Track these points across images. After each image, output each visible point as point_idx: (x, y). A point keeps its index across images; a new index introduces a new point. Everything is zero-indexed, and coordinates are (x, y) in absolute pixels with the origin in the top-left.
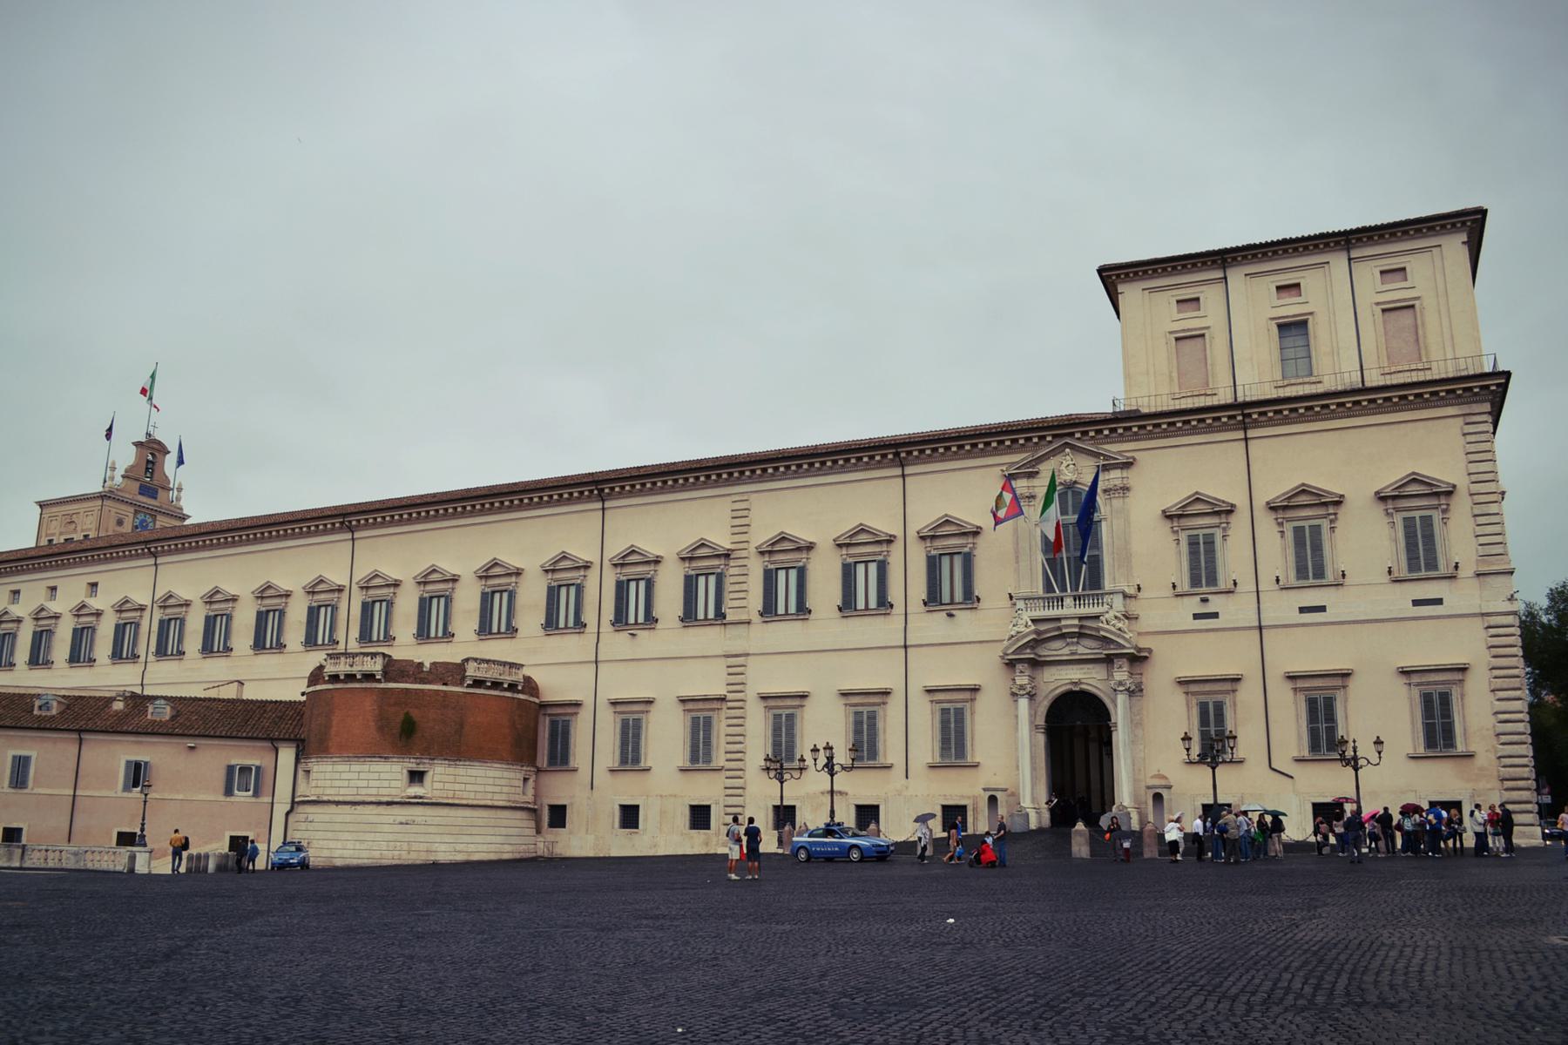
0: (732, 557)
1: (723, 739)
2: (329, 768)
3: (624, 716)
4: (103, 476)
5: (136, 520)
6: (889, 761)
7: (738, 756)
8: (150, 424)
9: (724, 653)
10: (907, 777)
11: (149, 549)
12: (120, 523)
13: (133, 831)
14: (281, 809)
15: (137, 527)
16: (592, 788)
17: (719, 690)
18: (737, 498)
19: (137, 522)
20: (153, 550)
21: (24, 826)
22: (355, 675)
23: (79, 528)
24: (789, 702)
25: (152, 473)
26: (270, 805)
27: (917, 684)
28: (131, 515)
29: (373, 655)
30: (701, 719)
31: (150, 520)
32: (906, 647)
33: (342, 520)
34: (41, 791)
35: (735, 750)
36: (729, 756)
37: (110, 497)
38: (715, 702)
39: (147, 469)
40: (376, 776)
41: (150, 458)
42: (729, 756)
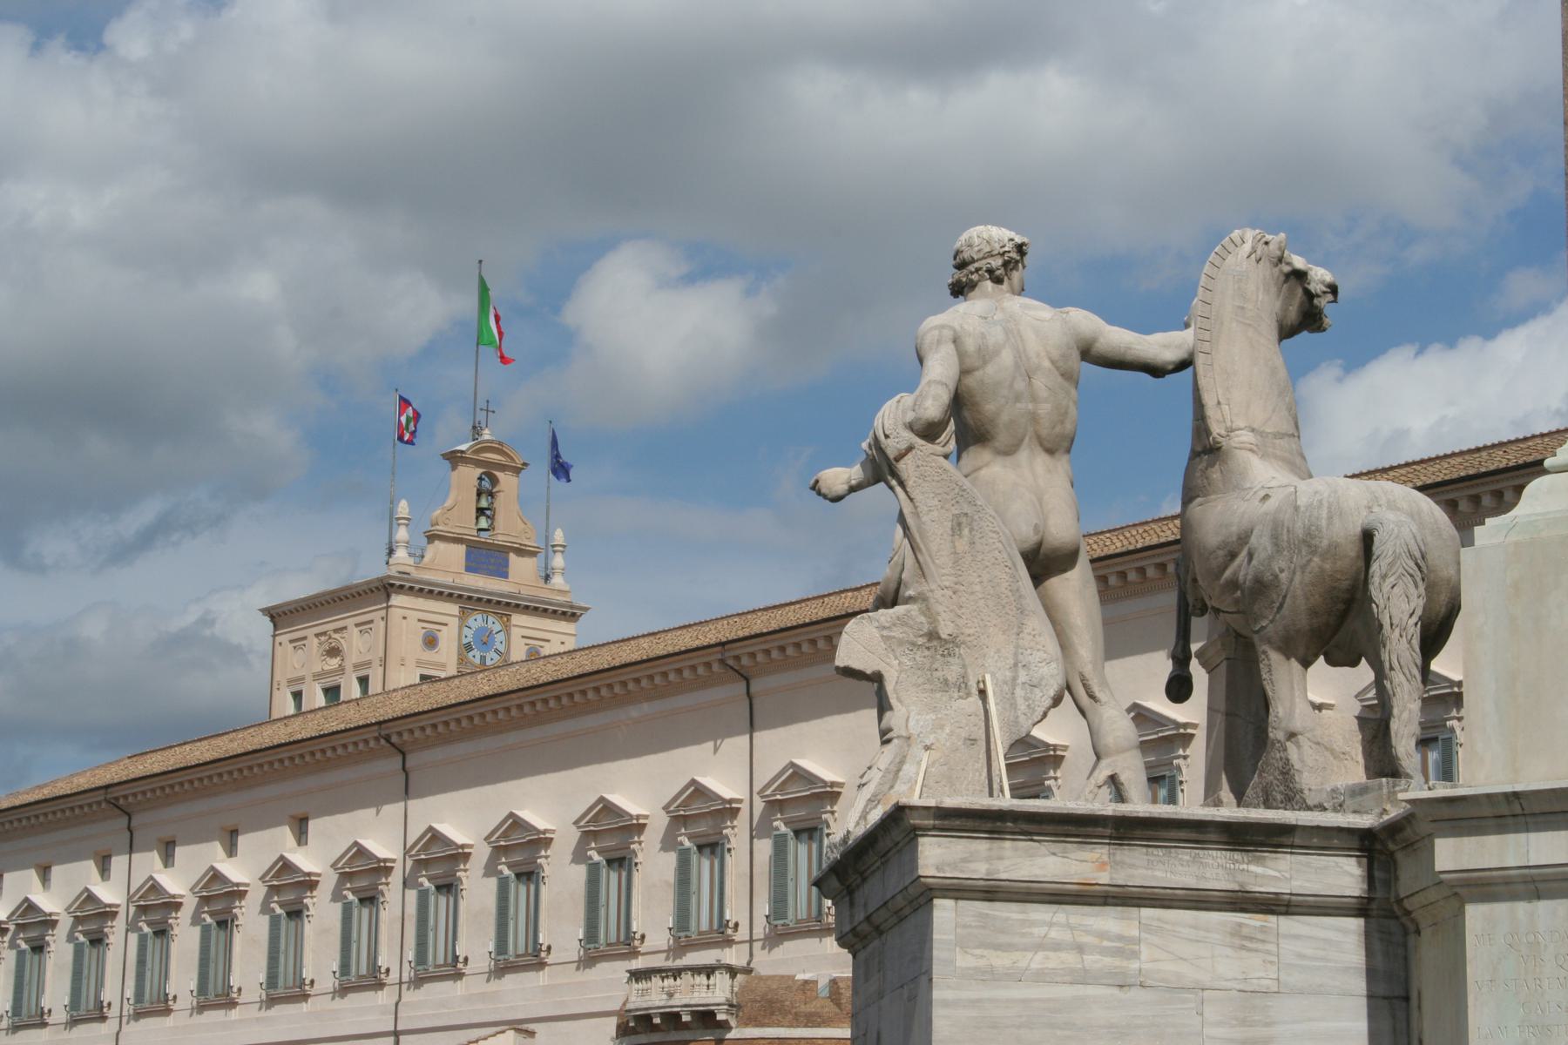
4: (387, 541)
8: (478, 407)
11: (387, 739)
12: (431, 642)
15: (468, 647)
19: (469, 633)
20: (394, 739)
22: (677, 1016)
23: (348, 665)
25: (491, 518)
28: (454, 622)
29: (709, 971)
31: (497, 627)
33: (719, 656)
37: (402, 587)
39: (480, 511)
41: (486, 484)
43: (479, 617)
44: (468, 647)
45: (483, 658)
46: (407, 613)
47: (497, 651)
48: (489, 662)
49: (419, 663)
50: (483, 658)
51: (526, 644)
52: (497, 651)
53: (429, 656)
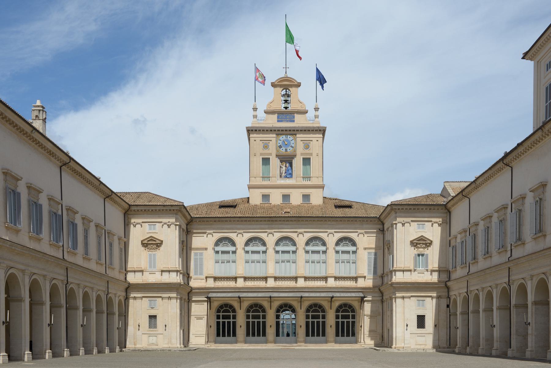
5: (279, 141)
12: (266, 147)
15: (280, 147)
19: (281, 142)
28: (274, 140)
31: (291, 138)
37: (252, 130)
43: (284, 136)
44: (280, 147)
45: (286, 150)
46: (255, 139)
47: (292, 147)
48: (288, 150)
49: (261, 154)
50: (286, 150)
51: (303, 143)
52: (292, 147)
53: (266, 151)
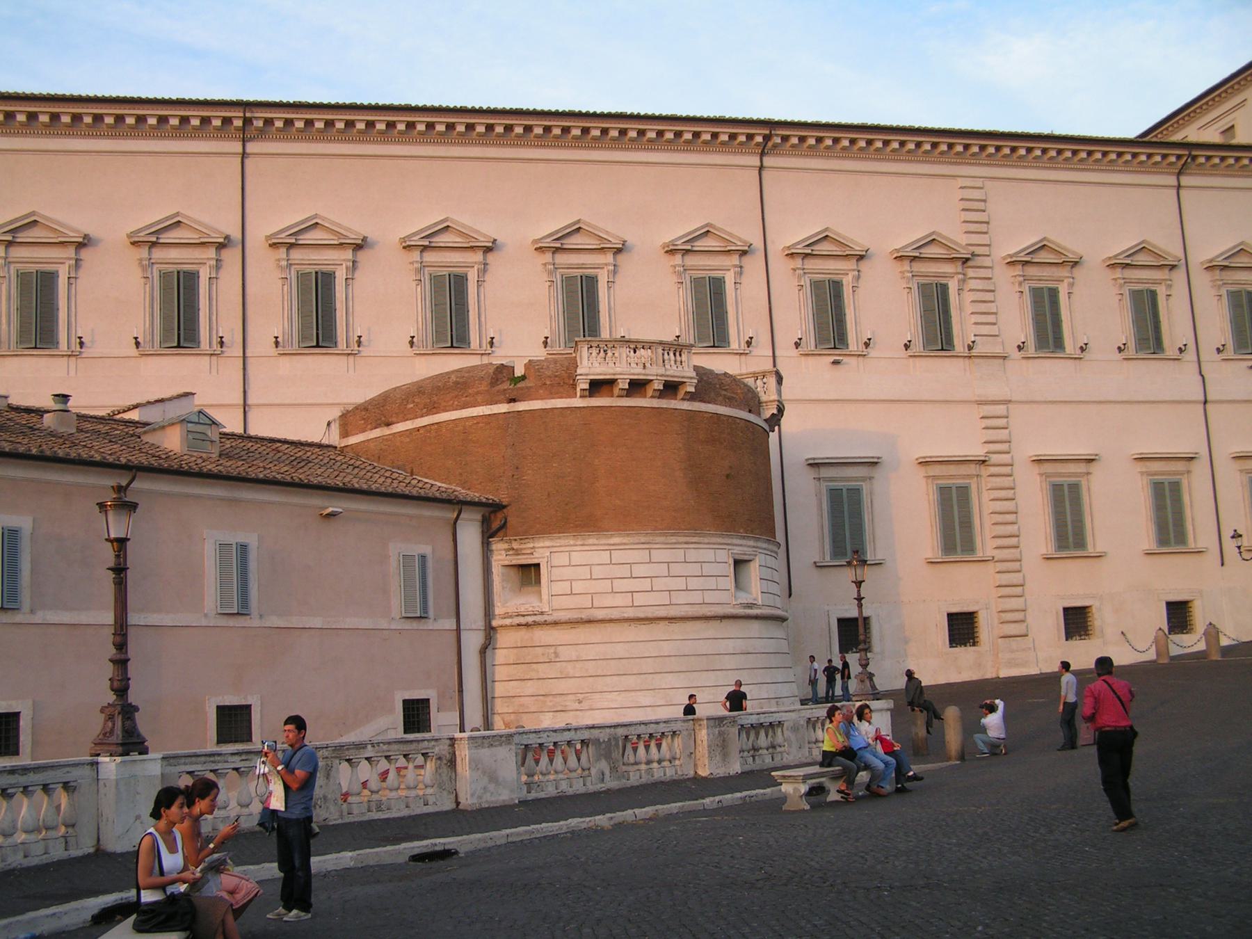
0: (970, 263)
1: (988, 521)
2: (605, 557)
3: (833, 485)
6: (1201, 545)
7: (1012, 540)
9: (978, 399)
10: (1222, 565)
13: (243, 703)
14: (472, 641)
16: (790, 595)
17: (978, 451)
18: (968, 182)
21: (253, 700)
24: (1072, 468)
26: (454, 635)
27: (1227, 446)
30: (954, 491)
32: (1205, 402)
34: (52, 617)
35: (1008, 533)
36: (1000, 542)
38: (973, 466)
40: (625, 571)
42: (1000, 542)
